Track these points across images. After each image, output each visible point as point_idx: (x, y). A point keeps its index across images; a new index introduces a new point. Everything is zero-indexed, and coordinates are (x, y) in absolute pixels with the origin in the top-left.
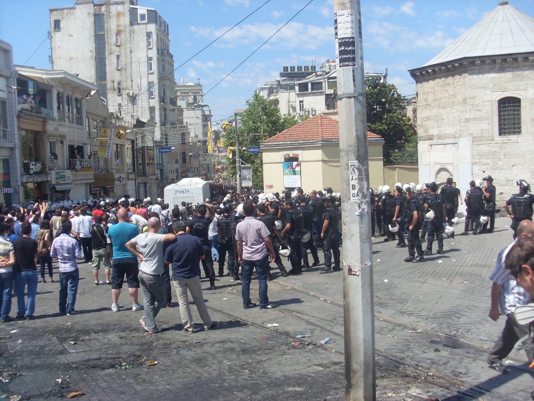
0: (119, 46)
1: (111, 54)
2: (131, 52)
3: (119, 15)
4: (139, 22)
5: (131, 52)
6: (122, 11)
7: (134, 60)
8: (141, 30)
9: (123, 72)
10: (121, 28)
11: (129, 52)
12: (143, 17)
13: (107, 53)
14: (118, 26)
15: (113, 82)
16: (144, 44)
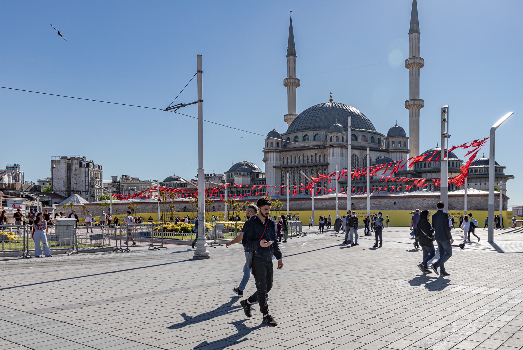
0: (76, 175)
1: (73, 178)
2: (80, 178)
3: (76, 164)
4: (83, 167)
5: (80, 178)
6: (77, 163)
7: (81, 180)
8: (83, 169)
9: (77, 185)
10: (77, 169)
11: (79, 178)
12: (84, 165)
13: (71, 178)
14: (75, 168)
15: (73, 188)
16: (84, 176)
